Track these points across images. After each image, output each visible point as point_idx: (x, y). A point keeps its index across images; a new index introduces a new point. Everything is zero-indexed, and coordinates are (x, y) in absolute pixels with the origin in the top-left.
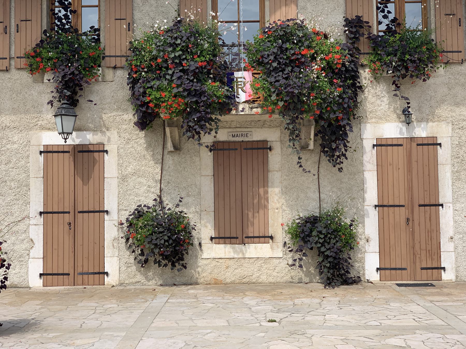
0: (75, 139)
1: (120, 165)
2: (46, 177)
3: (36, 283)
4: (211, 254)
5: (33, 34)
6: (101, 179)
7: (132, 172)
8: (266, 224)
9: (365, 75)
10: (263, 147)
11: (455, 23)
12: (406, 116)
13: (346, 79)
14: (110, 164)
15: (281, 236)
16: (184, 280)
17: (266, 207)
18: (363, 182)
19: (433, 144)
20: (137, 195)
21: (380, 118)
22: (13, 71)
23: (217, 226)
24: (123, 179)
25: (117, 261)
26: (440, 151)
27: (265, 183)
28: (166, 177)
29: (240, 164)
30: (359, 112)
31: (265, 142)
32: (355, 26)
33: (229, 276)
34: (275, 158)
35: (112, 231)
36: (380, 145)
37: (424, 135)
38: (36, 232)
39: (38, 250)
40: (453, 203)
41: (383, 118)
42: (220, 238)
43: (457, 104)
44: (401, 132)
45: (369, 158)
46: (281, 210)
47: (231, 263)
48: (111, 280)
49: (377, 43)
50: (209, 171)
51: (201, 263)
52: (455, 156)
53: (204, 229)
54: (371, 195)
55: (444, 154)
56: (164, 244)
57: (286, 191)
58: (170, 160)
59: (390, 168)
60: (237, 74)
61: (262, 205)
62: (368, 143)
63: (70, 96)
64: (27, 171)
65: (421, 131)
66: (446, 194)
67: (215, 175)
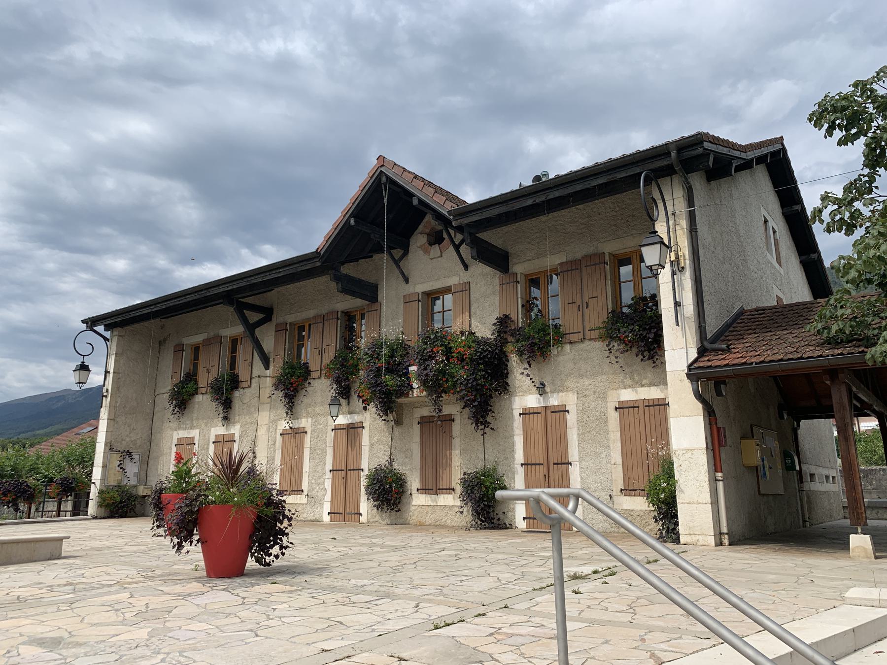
0: (342, 420)
2: (334, 446)
3: (327, 519)
4: (419, 500)
5: (330, 355)
6: (361, 446)
7: (377, 442)
8: (450, 478)
9: (514, 359)
10: (450, 419)
11: (576, 309)
12: (541, 389)
13: (479, 364)
15: (459, 489)
16: (401, 521)
17: (450, 466)
18: (513, 444)
19: (562, 410)
20: (378, 458)
23: (421, 481)
24: (371, 446)
25: (365, 506)
26: (568, 416)
27: (450, 447)
30: (511, 389)
31: (450, 415)
32: (503, 322)
33: (428, 519)
34: (456, 428)
35: (364, 482)
36: (526, 413)
37: (556, 404)
38: (328, 484)
39: (328, 497)
40: (580, 462)
41: (526, 392)
42: (424, 490)
43: (581, 376)
44: (539, 402)
45: (518, 423)
46: (459, 467)
47: (429, 509)
48: (363, 519)
49: (518, 333)
50: (417, 438)
51: (412, 508)
53: (414, 483)
54: (519, 456)
55: (571, 419)
56: (388, 492)
58: (397, 431)
59: (532, 432)
61: (448, 465)
63: (344, 392)
64: (325, 443)
65: (554, 401)
66: (574, 454)
67: (421, 442)
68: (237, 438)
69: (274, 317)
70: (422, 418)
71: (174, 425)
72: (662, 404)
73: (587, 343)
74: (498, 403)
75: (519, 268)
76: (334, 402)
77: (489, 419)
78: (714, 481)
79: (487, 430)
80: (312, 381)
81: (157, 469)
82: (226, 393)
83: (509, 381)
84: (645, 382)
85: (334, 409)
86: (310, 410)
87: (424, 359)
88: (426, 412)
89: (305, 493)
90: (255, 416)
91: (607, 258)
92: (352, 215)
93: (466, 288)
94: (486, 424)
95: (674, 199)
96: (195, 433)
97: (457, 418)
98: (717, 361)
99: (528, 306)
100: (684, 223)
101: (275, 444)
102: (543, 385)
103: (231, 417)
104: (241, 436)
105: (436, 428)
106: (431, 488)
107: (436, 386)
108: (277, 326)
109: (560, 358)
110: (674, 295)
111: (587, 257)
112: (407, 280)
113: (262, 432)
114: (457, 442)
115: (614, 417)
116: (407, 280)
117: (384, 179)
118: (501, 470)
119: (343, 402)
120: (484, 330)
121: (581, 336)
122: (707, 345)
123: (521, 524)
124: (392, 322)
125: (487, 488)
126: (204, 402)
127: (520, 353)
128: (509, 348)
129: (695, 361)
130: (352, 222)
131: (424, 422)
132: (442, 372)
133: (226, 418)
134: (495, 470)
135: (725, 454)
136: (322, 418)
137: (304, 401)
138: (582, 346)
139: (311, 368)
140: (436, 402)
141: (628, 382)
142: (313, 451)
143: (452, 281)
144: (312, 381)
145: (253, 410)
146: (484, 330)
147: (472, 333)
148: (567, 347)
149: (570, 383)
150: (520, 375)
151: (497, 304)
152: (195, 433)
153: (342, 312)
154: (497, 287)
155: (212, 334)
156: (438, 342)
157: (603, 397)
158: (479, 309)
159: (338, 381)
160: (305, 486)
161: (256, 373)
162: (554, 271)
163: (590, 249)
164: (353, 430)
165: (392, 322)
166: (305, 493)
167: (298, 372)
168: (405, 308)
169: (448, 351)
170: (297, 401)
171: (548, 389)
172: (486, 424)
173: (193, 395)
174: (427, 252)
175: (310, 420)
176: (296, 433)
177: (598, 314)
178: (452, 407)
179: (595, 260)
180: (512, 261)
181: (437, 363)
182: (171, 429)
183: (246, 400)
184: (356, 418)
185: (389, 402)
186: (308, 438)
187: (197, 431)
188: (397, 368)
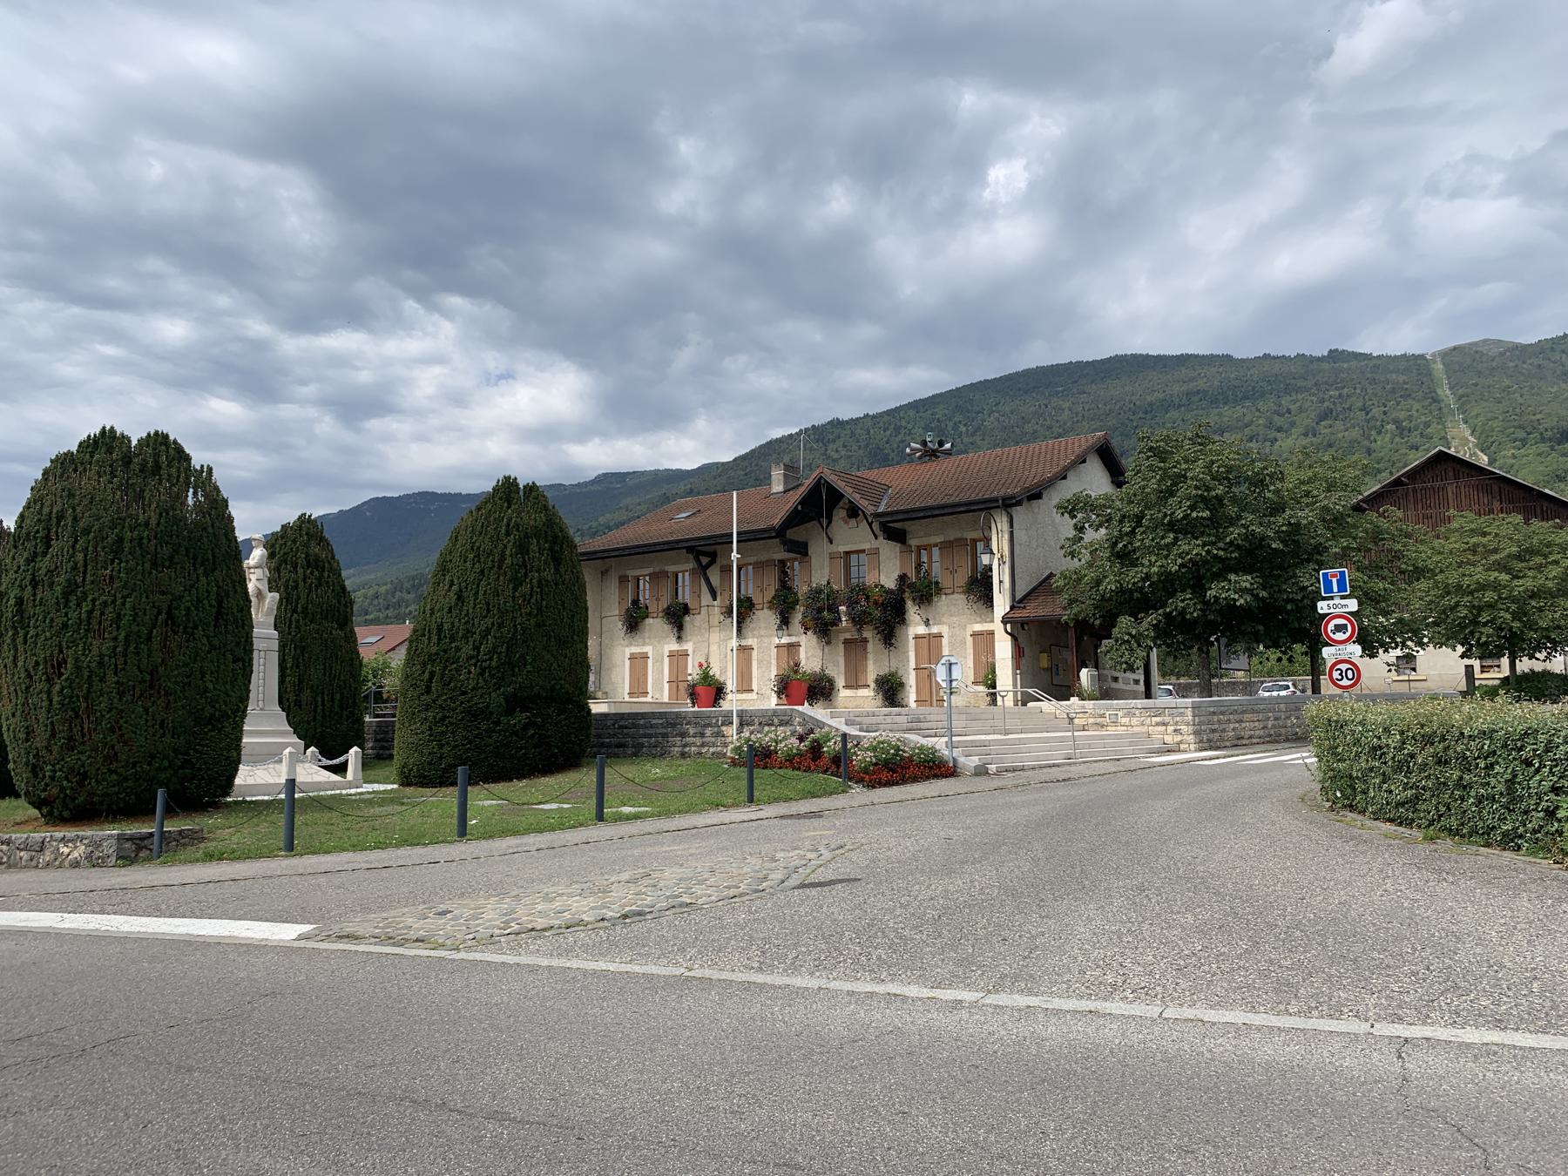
0: (785, 640)
4: (843, 694)
5: (770, 593)
9: (909, 603)
10: (865, 641)
12: (927, 623)
14: (802, 650)
15: (873, 685)
29: (855, 648)
34: (870, 647)
36: (917, 637)
46: (872, 672)
49: (911, 586)
53: (840, 682)
54: (912, 664)
55: (945, 641)
57: (875, 662)
63: (785, 622)
65: (935, 630)
72: (992, 633)
74: (899, 631)
75: (913, 542)
76: (780, 628)
78: (1015, 675)
82: (677, 617)
87: (852, 604)
88: (848, 636)
93: (875, 552)
94: (891, 645)
96: (648, 649)
98: (1018, 614)
99: (919, 566)
100: (1006, 536)
105: (855, 648)
107: (859, 621)
110: (1001, 577)
111: (957, 540)
113: (714, 648)
114: (870, 656)
115: (970, 640)
120: (889, 581)
123: (913, 705)
124: (819, 573)
126: (656, 625)
131: (846, 642)
135: (1023, 661)
137: (749, 625)
140: (859, 630)
143: (866, 546)
150: (912, 611)
152: (648, 649)
156: (858, 593)
158: (887, 572)
161: (704, 603)
164: (792, 647)
169: (868, 597)
172: (891, 645)
176: (744, 650)
177: (962, 577)
178: (868, 633)
179: (961, 542)
184: (793, 639)
185: (823, 628)
186: (755, 653)
188: (833, 609)
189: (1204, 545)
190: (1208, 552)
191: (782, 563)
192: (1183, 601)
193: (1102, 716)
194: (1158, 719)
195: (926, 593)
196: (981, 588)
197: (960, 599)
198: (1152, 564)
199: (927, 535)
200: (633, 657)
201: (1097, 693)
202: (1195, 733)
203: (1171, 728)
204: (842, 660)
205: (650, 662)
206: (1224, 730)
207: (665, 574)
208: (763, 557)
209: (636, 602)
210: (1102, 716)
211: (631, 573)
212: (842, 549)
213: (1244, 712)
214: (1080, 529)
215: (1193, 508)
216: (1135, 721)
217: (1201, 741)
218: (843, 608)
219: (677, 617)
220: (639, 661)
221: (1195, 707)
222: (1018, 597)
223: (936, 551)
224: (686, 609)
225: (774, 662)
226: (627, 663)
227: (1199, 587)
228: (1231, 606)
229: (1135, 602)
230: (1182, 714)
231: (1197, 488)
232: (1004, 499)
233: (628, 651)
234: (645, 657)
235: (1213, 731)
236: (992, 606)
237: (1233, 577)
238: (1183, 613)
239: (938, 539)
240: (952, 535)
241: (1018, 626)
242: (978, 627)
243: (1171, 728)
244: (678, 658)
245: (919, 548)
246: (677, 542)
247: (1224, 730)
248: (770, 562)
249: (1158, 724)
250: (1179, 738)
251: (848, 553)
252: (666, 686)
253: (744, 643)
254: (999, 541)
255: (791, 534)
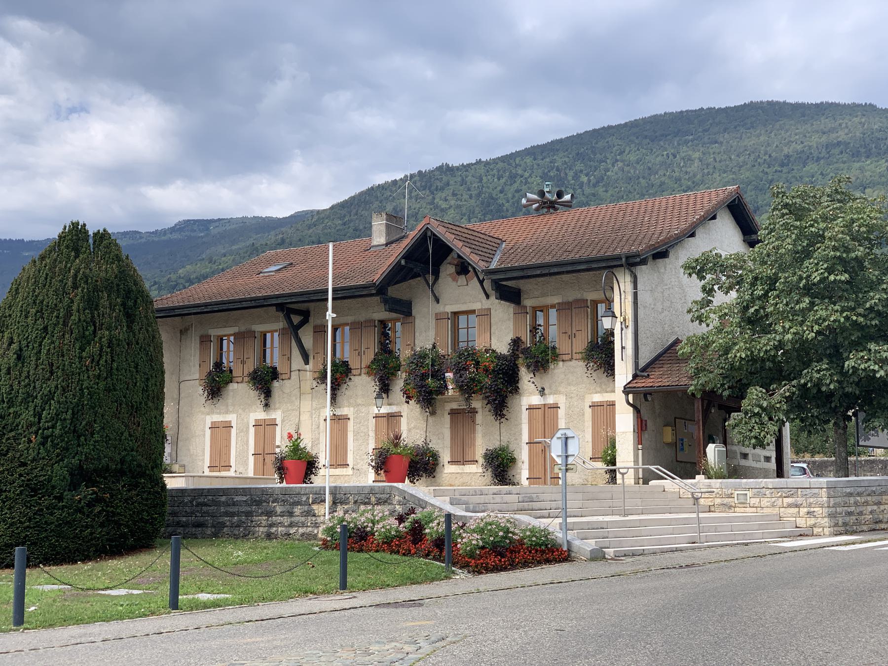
0: (384, 410)
1: (408, 423)
4: (448, 470)
5: (369, 357)
8: (474, 454)
10: (474, 411)
12: (542, 392)
13: (499, 374)
14: (404, 421)
15: (481, 461)
17: (474, 445)
19: (556, 407)
21: (529, 395)
22: (363, 375)
23: (452, 456)
27: (474, 431)
28: (429, 430)
34: (479, 418)
36: (530, 408)
41: (531, 394)
43: (569, 384)
49: (526, 351)
50: (449, 426)
51: (444, 475)
52: (567, 414)
53: (445, 457)
54: (525, 438)
55: (561, 413)
60: (446, 375)
61: (473, 444)
62: (524, 408)
63: (385, 389)
65: (550, 400)
67: (451, 427)
68: (278, 422)
69: (311, 319)
70: (452, 410)
71: (207, 410)
73: (574, 361)
74: (512, 401)
75: (528, 303)
76: (379, 396)
77: (504, 412)
78: (636, 450)
79: (502, 420)
80: (352, 377)
81: (189, 450)
82: (265, 381)
83: (520, 385)
84: (608, 390)
85: (379, 401)
86: (351, 401)
87: (459, 370)
88: (455, 406)
89: (351, 466)
90: (297, 403)
91: (589, 304)
92: (403, 257)
93: (486, 314)
94: (502, 416)
95: (623, 284)
96: (232, 418)
97: (480, 411)
98: (641, 383)
99: (534, 329)
100: (630, 298)
101: (318, 427)
102: (543, 389)
103: (271, 405)
104: (283, 421)
105: (462, 419)
106: (459, 460)
107: (467, 389)
108: (315, 327)
109: (556, 371)
110: (623, 342)
111: (577, 301)
112: (438, 301)
113: (305, 417)
114: (479, 429)
115: (588, 412)
116: (438, 301)
117: (429, 234)
118: (512, 447)
119: (384, 395)
120: (502, 347)
121: (570, 356)
122: (639, 373)
123: (525, 482)
124: (424, 335)
125: (503, 459)
126: (241, 391)
127: (528, 367)
128: (520, 361)
129: (629, 383)
130: (403, 262)
131: (453, 413)
132: (473, 379)
133: (267, 405)
134: (508, 447)
135: (646, 436)
136: (363, 406)
138: (570, 363)
139: (352, 366)
140: (468, 400)
141: (598, 389)
142: (356, 434)
143: (476, 306)
144: (352, 377)
145: (294, 398)
146: (502, 347)
147: (494, 351)
148: (561, 363)
149: (561, 389)
151: (512, 327)
153: (379, 321)
154: (512, 315)
155: (243, 329)
157: (582, 398)
158: (498, 332)
159: (381, 380)
160: (350, 460)
161: (295, 366)
162: (553, 306)
163: (579, 296)
164: (393, 417)
165: (424, 335)
166: (351, 466)
167: (341, 369)
168: (437, 325)
169: (477, 363)
170: (339, 393)
171: (546, 391)
172: (502, 416)
173: (227, 383)
174: (454, 280)
175: (352, 409)
176: (339, 420)
177: (581, 343)
178: (477, 403)
179: (581, 304)
180: (523, 296)
181: (470, 373)
182: (203, 413)
183: (287, 391)
184: (394, 409)
185: (427, 396)
186: (351, 424)
187: (235, 416)
188: (438, 375)
189: (842, 312)
190: (847, 318)
191: (383, 323)
192: (819, 372)
193: (730, 496)
194: (786, 500)
195: (542, 358)
196: (601, 354)
197: (578, 367)
198: (786, 331)
199: (544, 295)
200: (214, 427)
201: (724, 471)
202: (830, 516)
203: (803, 511)
204: (447, 433)
205: (234, 431)
206: (861, 513)
207: (251, 334)
208: (362, 317)
209: (218, 365)
210: (730, 496)
211: (214, 332)
212: (450, 309)
213: (881, 494)
214: (708, 291)
215: (830, 271)
216: (765, 502)
217: (836, 525)
218: (449, 375)
219: (265, 381)
220: (221, 430)
221: (830, 487)
222: (642, 364)
223: (553, 313)
224: (274, 374)
225: (372, 434)
226: (208, 432)
227: (836, 356)
228: (871, 377)
229: (767, 371)
230: (815, 495)
231: (835, 249)
232: (627, 258)
233: (210, 419)
234: (228, 426)
235: (850, 514)
236: (613, 375)
237: (872, 346)
238: (818, 384)
239: (556, 300)
240: (572, 295)
241: (641, 397)
242: (597, 398)
243: (803, 511)
244: (265, 428)
245: (535, 309)
246: (266, 298)
247: (861, 513)
248: (370, 323)
249: (790, 506)
250: (812, 521)
251: (456, 314)
252: (251, 459)
253: (338, 412)
254: (622, 303)
255: (394, 291)
